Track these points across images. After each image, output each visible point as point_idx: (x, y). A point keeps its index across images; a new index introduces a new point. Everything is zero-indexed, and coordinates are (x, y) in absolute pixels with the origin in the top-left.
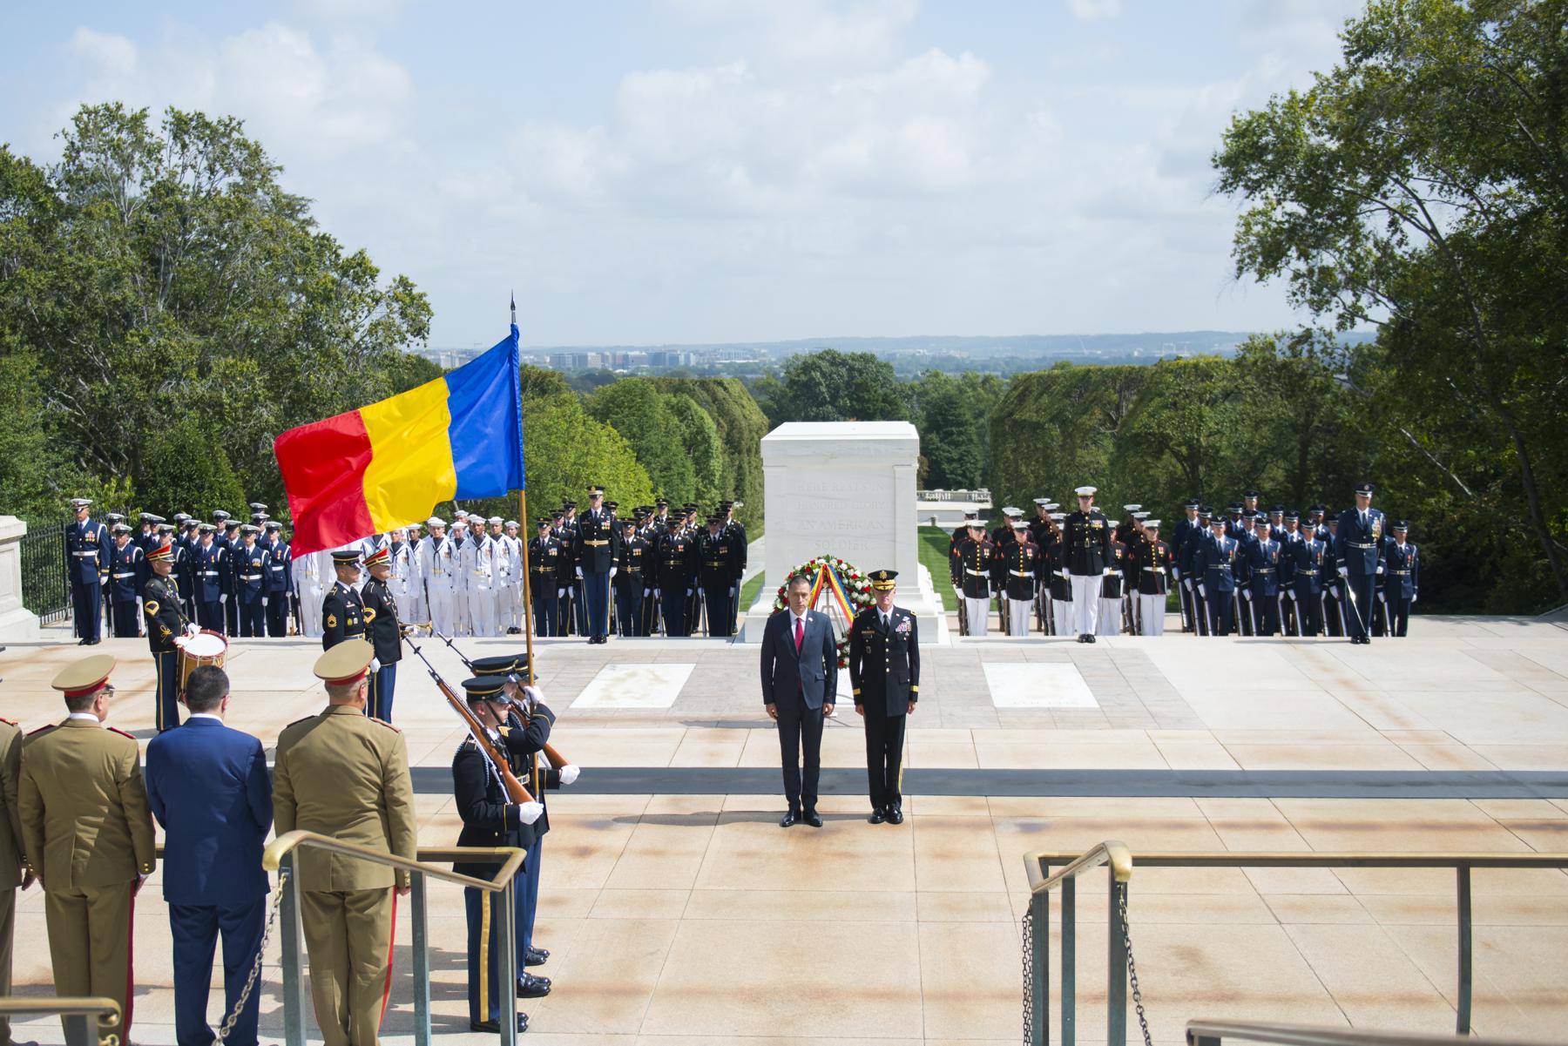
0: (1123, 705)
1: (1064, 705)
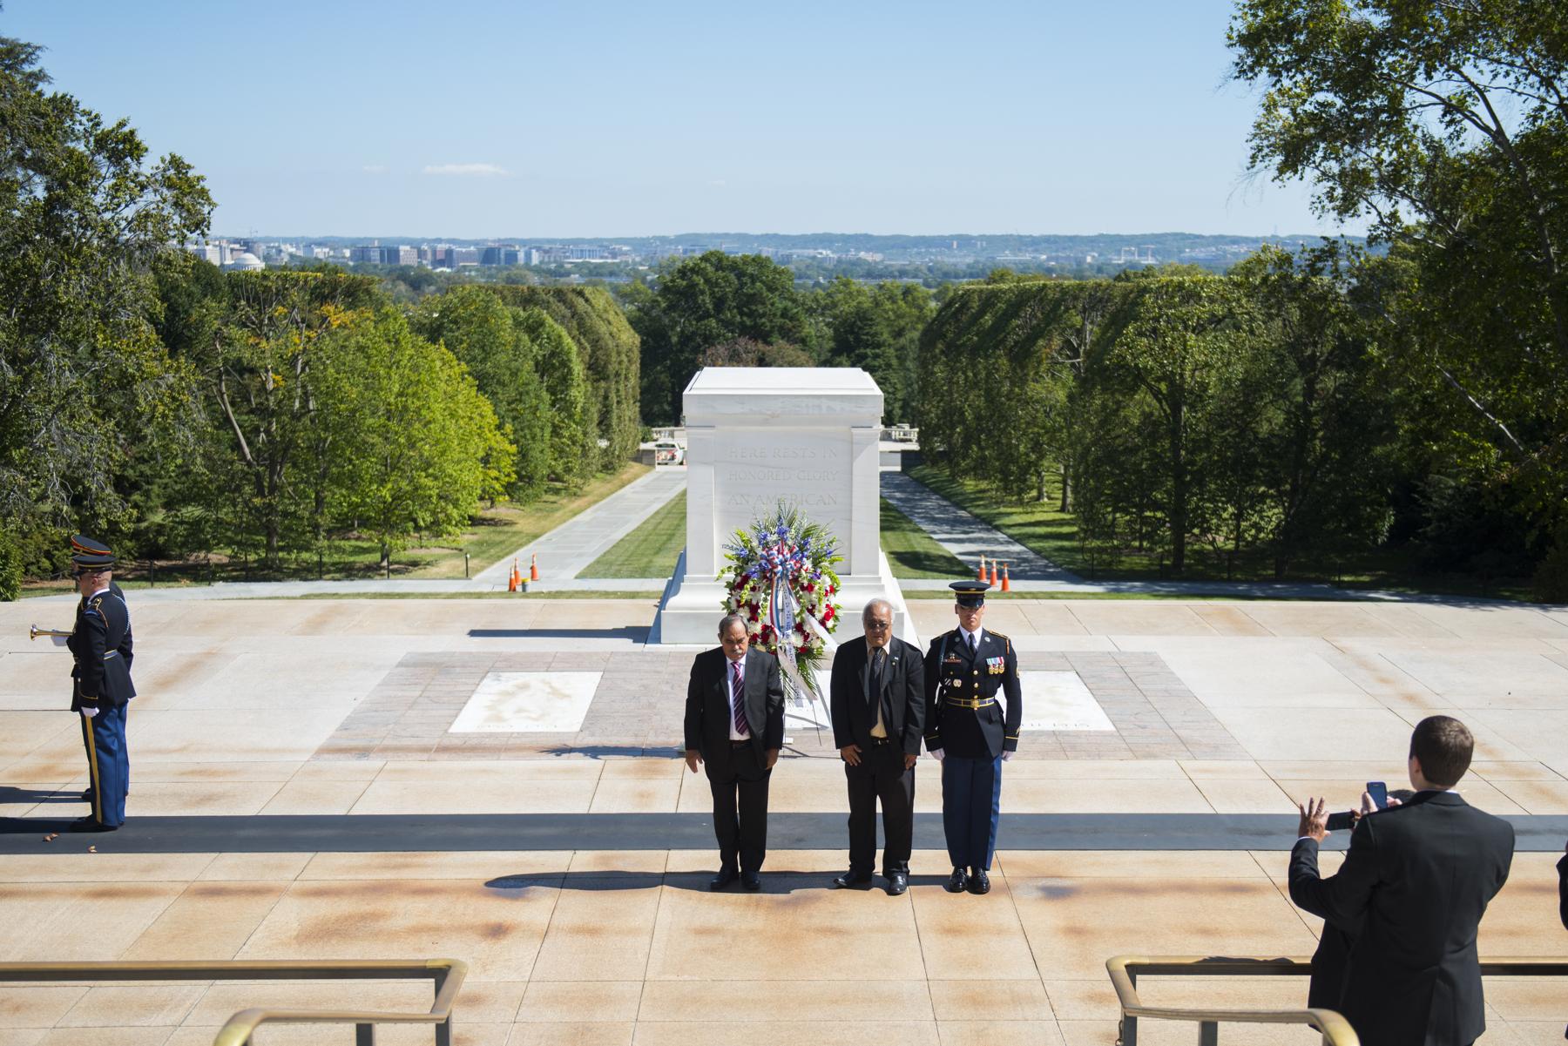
0: (1144, 728)
1: (1071, 728)
